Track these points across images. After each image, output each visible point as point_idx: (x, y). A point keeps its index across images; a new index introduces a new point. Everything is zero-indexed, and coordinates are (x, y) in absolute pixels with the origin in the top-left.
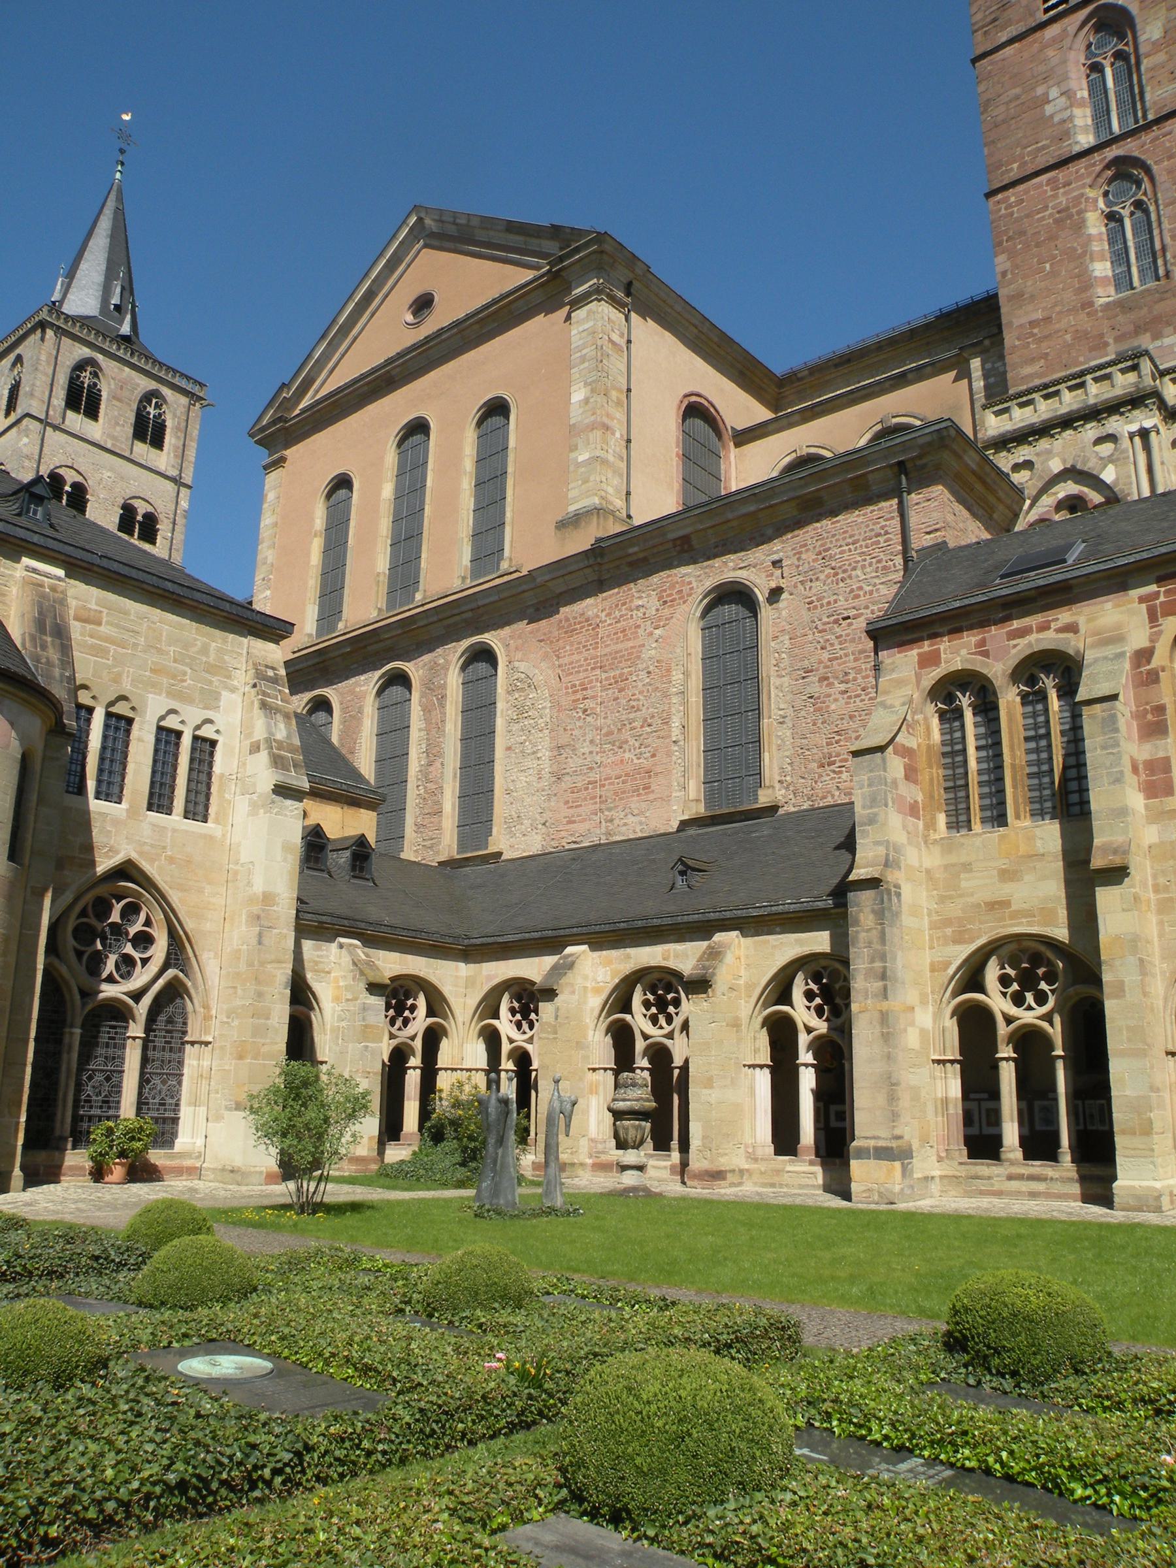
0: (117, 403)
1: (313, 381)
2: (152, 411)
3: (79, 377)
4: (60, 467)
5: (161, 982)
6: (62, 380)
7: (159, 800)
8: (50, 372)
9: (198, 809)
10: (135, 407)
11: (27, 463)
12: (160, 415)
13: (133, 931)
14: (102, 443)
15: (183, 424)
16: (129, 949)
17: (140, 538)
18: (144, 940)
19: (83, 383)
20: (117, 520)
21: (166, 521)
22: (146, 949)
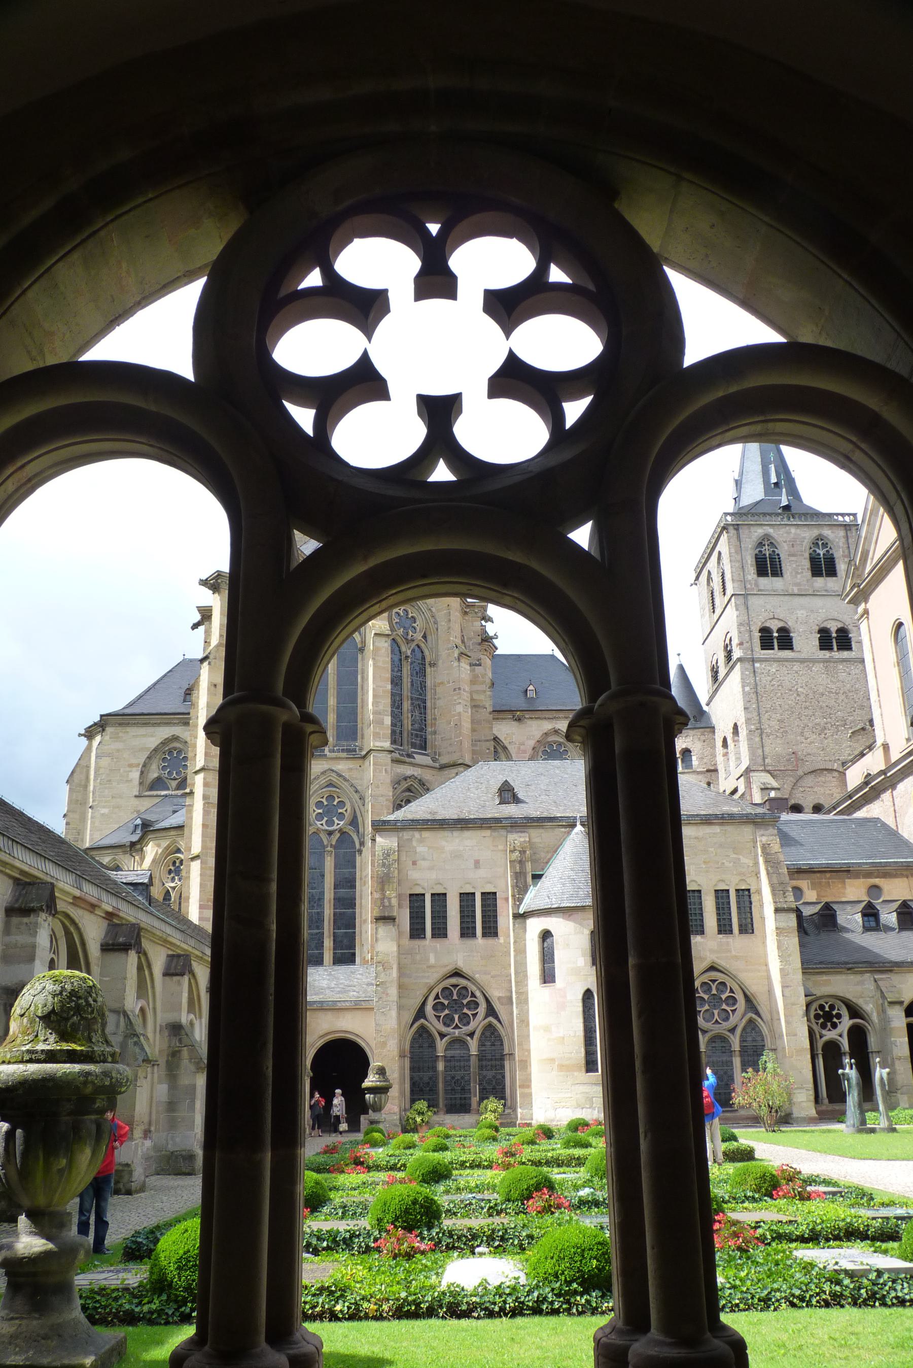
0: (793, 558)
1: (868, 552)
2: (821, 552)
3: (760, 551)
4: (766, 621)
5: (744, 1021)
6: (750, 561)
7: (724, 928)
8: (739, 558)
9: (747, 928)
10: (807, 555)
11: (743, 629)
12: (828, 551)
13: (724, 997)
14: (790, 592)
15: (847, 551)
16: (724, 1006)
17: (838, 649)
18: (732, 1000)
19: (765, 555)
20: (817, 643)
21: (855, 629)
22: (734, 1004)
